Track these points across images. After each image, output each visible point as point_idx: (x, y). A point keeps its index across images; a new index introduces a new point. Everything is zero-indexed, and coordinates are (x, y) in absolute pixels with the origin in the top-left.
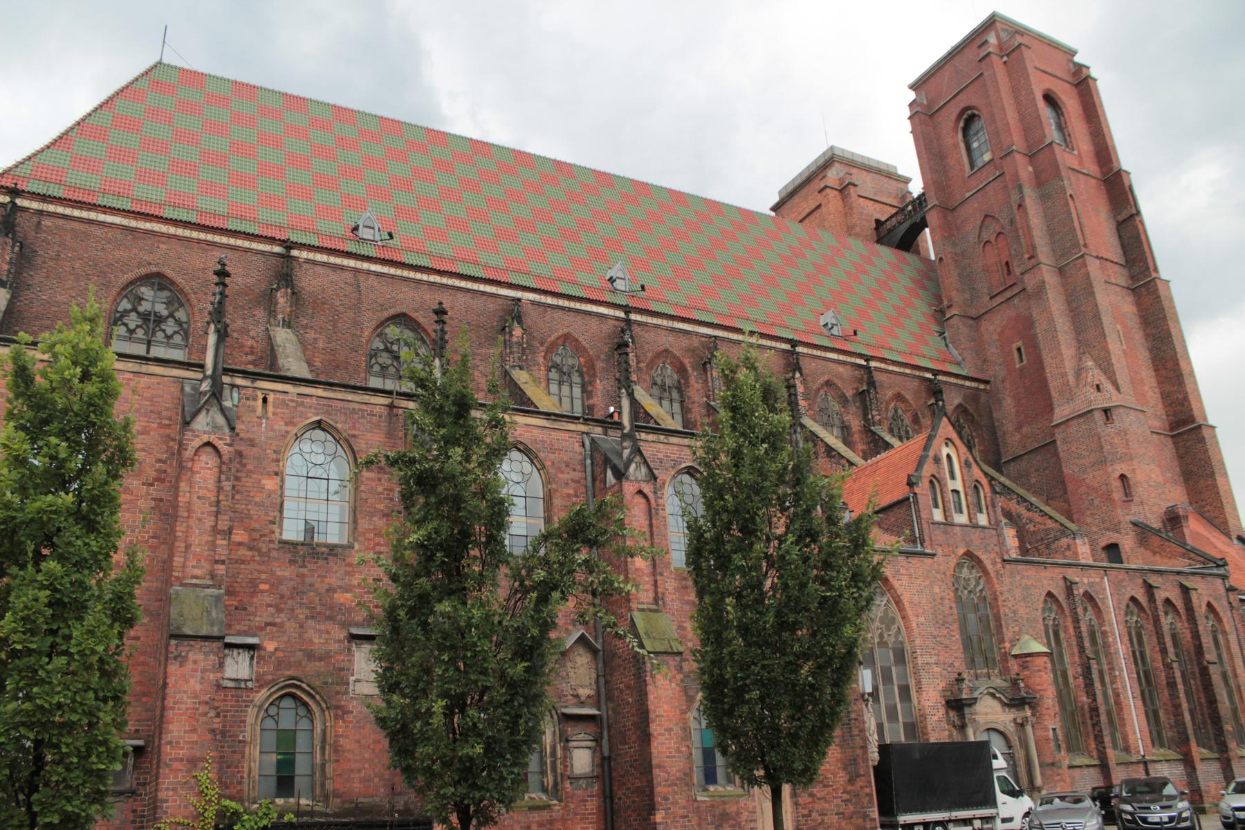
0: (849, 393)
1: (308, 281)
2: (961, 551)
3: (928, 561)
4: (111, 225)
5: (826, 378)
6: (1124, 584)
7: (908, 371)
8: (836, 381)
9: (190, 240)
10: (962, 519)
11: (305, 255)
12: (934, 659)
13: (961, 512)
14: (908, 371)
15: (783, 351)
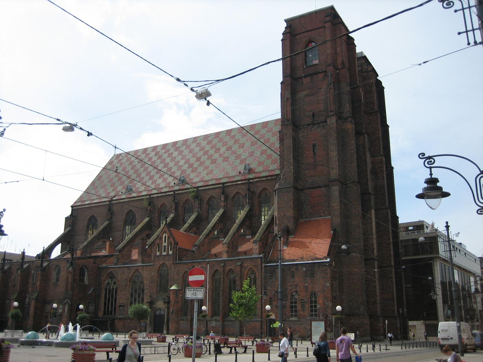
0: (244, 195)
1: (115, 208)
2: (161, 262)
3: (152, 267)
4: (87, 207)
5: (236, 191)
6: (215, 265)
7: (269, 178)
8: (240, 191)
9: (97, 206)
10: (165, 253)
11: (114, 202)
12: (148, 291)
13: (164, 251)
14: (269, 178)
15: (221, 187)
